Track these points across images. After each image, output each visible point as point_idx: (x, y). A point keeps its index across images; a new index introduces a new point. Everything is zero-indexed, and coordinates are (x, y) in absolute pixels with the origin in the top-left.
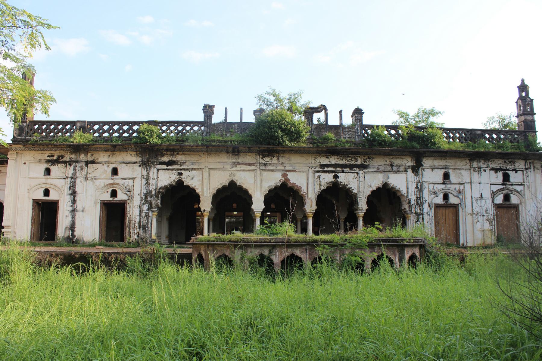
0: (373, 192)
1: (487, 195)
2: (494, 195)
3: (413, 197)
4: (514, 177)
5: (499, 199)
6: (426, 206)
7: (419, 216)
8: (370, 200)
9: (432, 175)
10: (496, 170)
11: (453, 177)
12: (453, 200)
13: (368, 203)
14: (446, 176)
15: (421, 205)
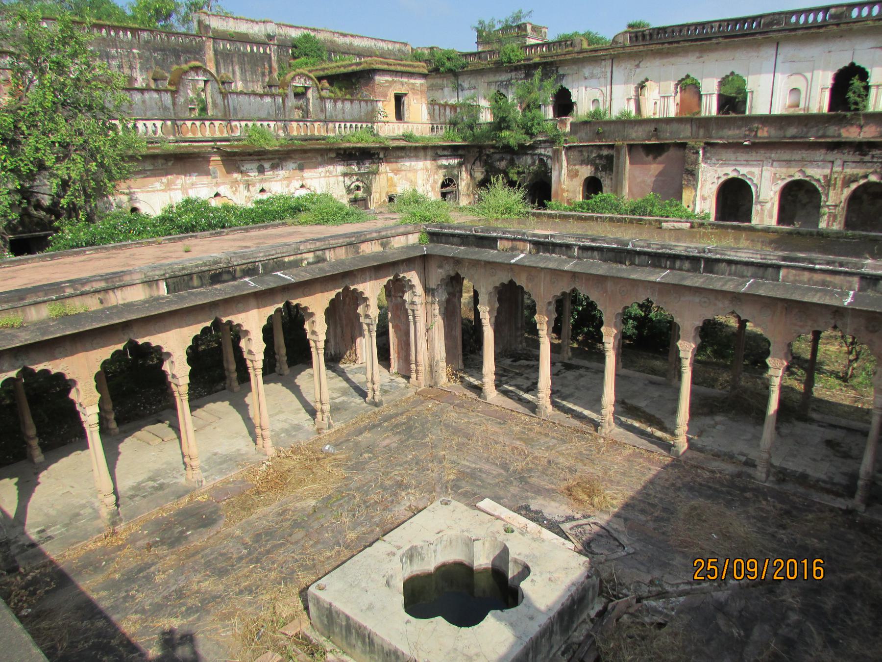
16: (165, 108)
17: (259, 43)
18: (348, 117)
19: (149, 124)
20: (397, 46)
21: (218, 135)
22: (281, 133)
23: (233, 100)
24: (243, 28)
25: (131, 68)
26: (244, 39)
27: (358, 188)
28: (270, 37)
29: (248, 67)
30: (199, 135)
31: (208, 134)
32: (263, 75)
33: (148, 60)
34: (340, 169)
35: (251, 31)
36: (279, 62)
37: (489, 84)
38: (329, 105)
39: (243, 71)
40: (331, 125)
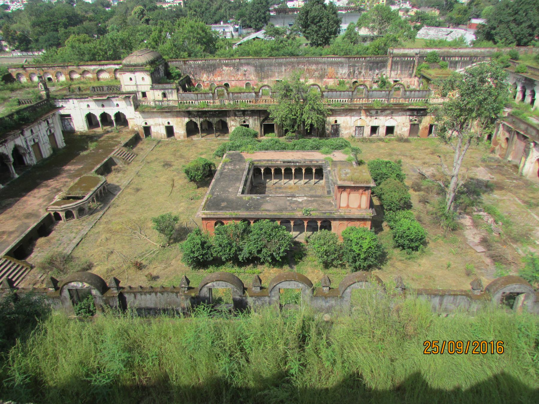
0: (13, 151)
1: (45, 133)
2: (47, 131)
3: (25, 146)
4: (50, 121)
5: (49, 134)
6: (30, 148)
7: (29, 153)
8: (13, 154)
9: (27, 133)
10: (44, 121)
11: (34, 131)
12: (37, 141)
13: (13, 157)
14: (32, 131)
15: (28, 148)
16: (350, 96)
17: (410, 57)
18: (416, 96)
19: (344, 100)
20: (488, 50)
21: (364, 102)
22: (386, 102)
23: (370, 93)
24: (406, 51)
25: (361, 69)
26: (405, 56)
27: (416, 120)
28: (416, 54)
29: (404, 65)
30: (358, 103)
31: (361, 102)
32: (410, 68)
33: (367, 66)
34: (408, 113)
35: (409, 52)
36: (419, 62)
37: (514, 77)
38: (408, 93)
39: (401, 67)
40: (407, 100)
